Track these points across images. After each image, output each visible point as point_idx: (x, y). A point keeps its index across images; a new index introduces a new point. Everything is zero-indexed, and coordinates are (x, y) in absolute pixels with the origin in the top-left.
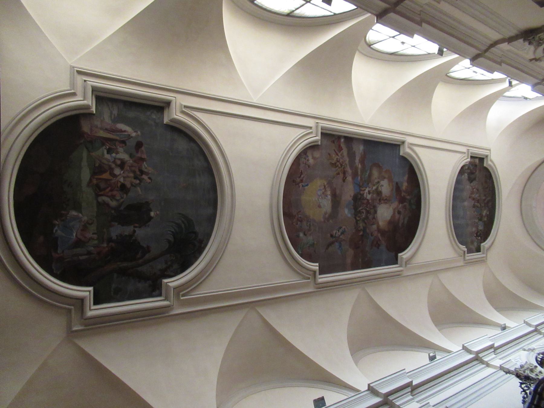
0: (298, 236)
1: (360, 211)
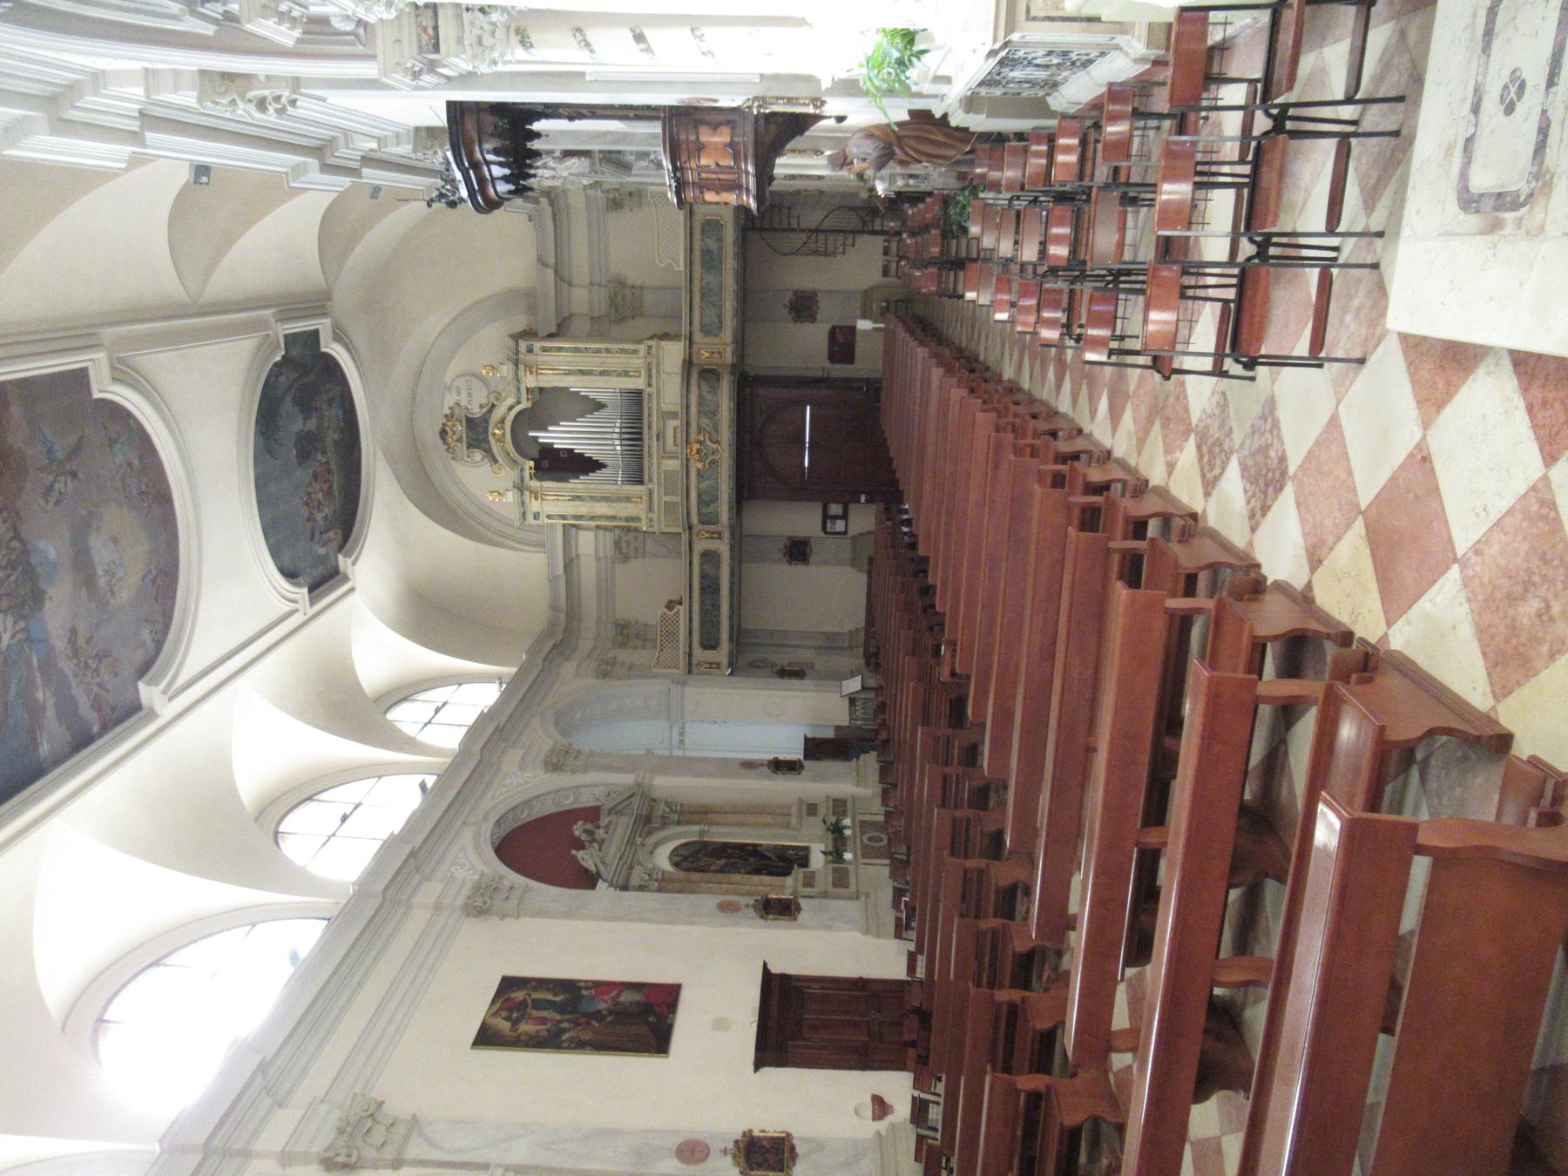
1: (14, 568)
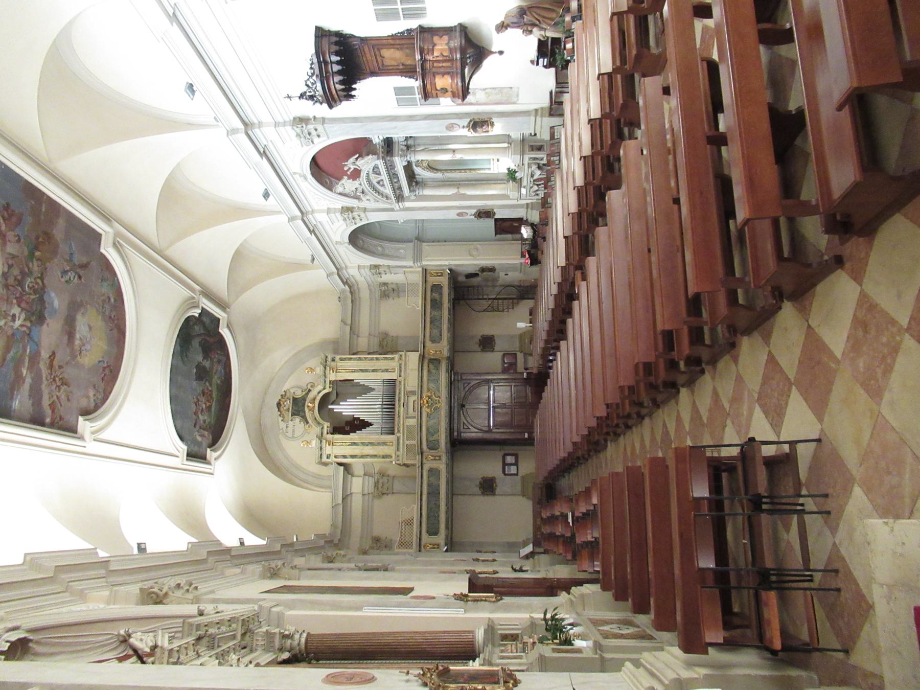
0: (115, 300)
